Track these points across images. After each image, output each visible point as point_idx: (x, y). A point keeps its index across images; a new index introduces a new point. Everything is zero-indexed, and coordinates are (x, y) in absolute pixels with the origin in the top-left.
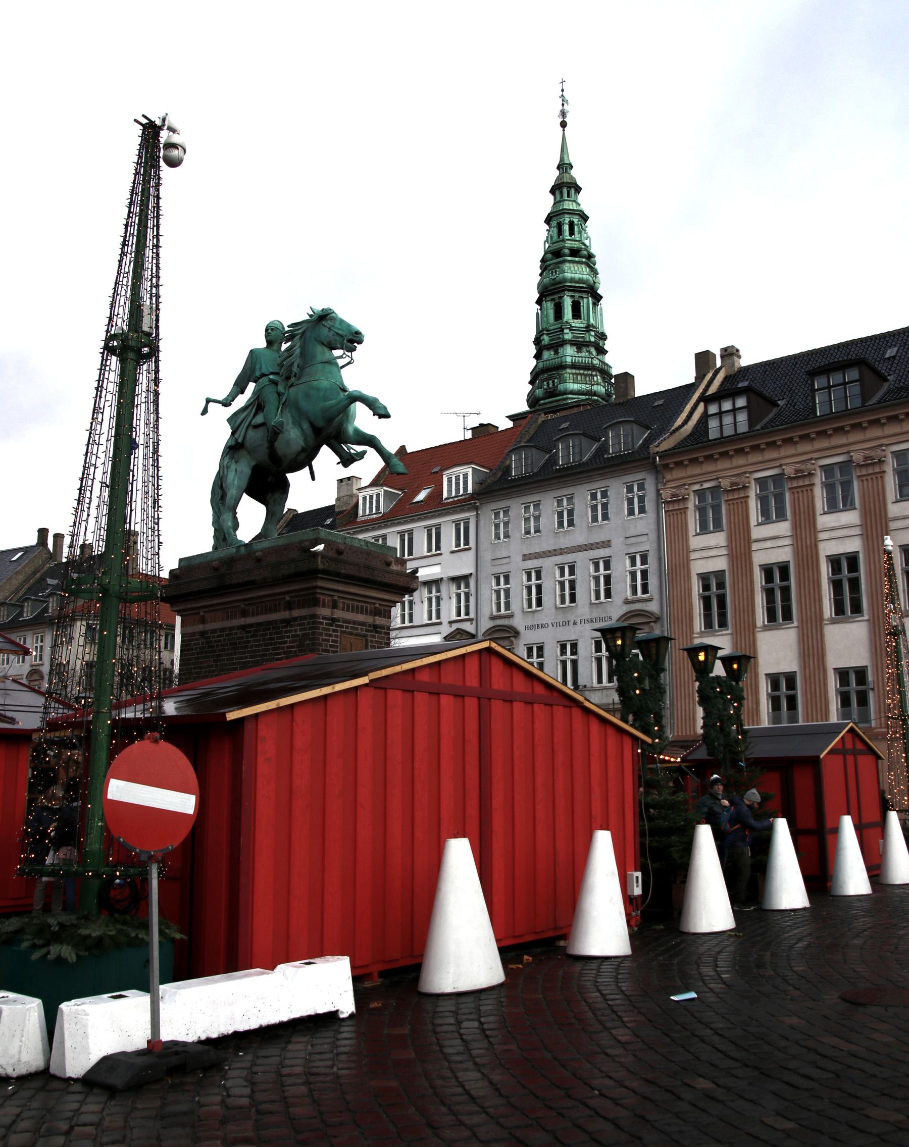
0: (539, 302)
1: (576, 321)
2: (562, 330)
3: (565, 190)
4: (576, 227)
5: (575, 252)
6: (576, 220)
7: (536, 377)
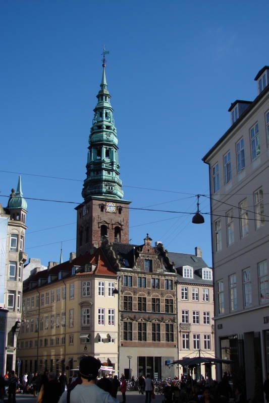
0: (90, 148)
3: (104, 97)
5: (108, 127)
7: (87, 184)
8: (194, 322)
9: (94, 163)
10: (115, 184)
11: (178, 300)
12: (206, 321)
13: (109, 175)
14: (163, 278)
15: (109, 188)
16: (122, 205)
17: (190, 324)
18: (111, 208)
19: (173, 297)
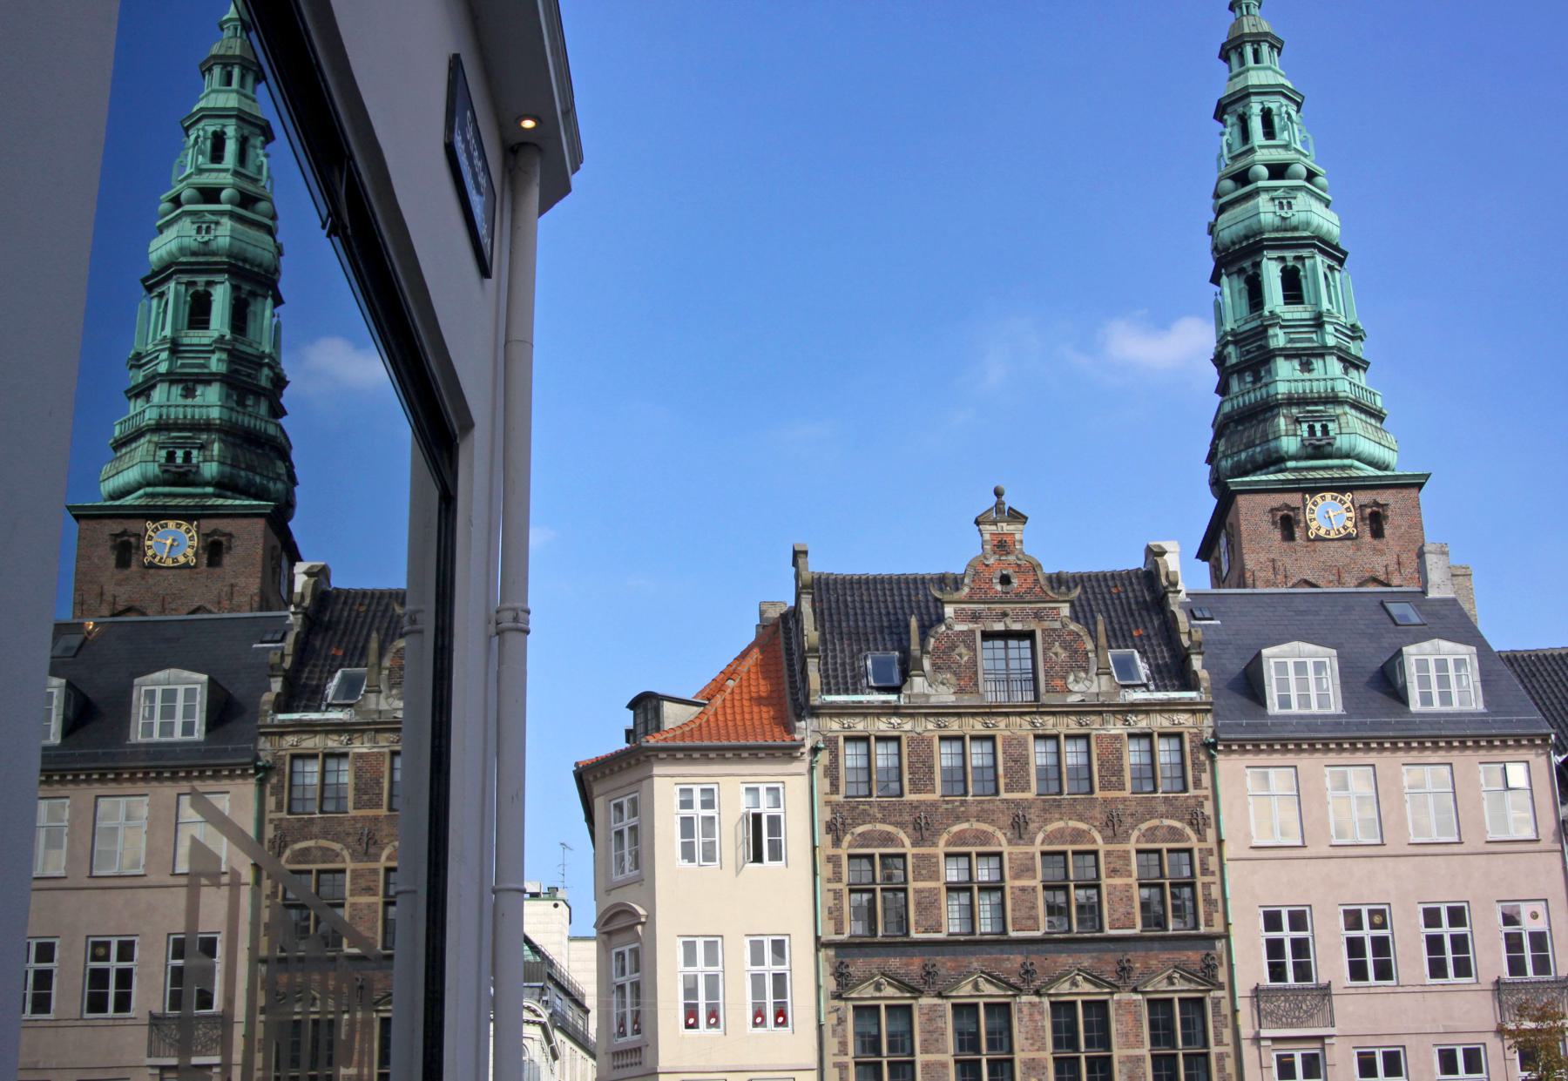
1: (1292, 307)
2: (1265, 329)
3: (1249, 50)
4: (1276, 119)
6: (1274, 106)
8: (1358, 972)
9: (1239, 339)
10: (1339, 410)
11: (1226, 855)
12: (1449, 956)
13: (1307, 376)
14: (1116, 728)
15: (1311, 428)
16: (1383, 497)
17: (1325, 991)
18: (1330, 515)
19: (1188, 831)
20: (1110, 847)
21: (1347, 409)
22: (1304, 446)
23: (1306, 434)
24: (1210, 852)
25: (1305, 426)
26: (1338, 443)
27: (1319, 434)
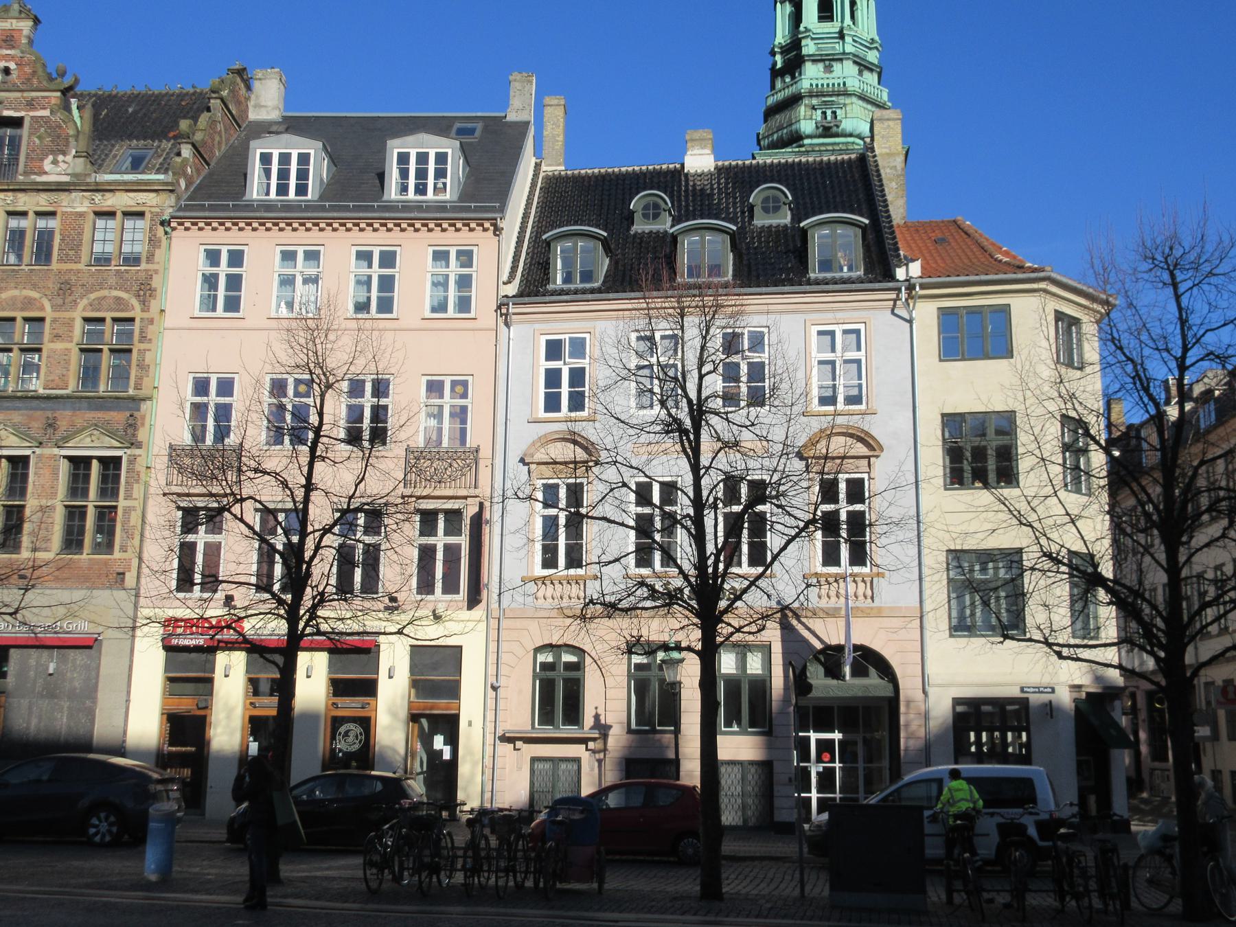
10: (848, 101)
13: (827, 75)
15: (824, 113)
20: (57, 315)
21: (854, 99)
22: (817, 127)
23: (819, 119)
24: (151, 321)
25: (819, 112)
26: (843, 126)
27: (829, 118)
